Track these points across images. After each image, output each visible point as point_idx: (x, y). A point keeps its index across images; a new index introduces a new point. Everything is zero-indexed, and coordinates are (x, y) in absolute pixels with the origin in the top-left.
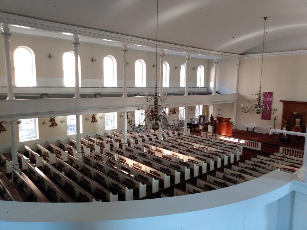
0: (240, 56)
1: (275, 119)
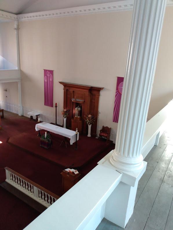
0: (15, 16)
1: (56, 107)
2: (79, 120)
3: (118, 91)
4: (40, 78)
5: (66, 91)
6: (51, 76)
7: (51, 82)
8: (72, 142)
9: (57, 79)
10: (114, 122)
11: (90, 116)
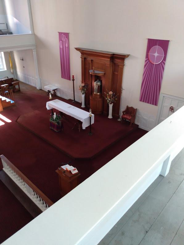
1: (73, 80)
2: (98, 97)
3: (148, 59)
5: (84, 60)
6: (67, 40)
7: (67, 49)
8: (85, 126)
9: (74, 43)
10: (140, 102)
11: (111, 93)
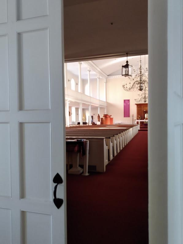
4: (121, 105)
